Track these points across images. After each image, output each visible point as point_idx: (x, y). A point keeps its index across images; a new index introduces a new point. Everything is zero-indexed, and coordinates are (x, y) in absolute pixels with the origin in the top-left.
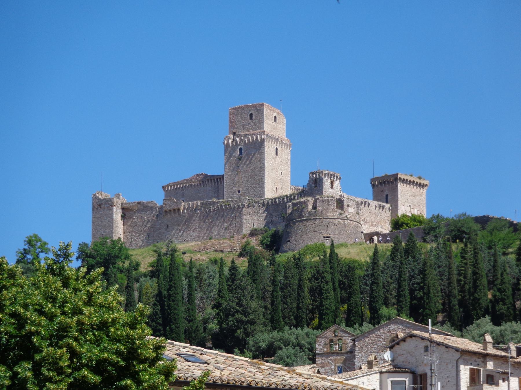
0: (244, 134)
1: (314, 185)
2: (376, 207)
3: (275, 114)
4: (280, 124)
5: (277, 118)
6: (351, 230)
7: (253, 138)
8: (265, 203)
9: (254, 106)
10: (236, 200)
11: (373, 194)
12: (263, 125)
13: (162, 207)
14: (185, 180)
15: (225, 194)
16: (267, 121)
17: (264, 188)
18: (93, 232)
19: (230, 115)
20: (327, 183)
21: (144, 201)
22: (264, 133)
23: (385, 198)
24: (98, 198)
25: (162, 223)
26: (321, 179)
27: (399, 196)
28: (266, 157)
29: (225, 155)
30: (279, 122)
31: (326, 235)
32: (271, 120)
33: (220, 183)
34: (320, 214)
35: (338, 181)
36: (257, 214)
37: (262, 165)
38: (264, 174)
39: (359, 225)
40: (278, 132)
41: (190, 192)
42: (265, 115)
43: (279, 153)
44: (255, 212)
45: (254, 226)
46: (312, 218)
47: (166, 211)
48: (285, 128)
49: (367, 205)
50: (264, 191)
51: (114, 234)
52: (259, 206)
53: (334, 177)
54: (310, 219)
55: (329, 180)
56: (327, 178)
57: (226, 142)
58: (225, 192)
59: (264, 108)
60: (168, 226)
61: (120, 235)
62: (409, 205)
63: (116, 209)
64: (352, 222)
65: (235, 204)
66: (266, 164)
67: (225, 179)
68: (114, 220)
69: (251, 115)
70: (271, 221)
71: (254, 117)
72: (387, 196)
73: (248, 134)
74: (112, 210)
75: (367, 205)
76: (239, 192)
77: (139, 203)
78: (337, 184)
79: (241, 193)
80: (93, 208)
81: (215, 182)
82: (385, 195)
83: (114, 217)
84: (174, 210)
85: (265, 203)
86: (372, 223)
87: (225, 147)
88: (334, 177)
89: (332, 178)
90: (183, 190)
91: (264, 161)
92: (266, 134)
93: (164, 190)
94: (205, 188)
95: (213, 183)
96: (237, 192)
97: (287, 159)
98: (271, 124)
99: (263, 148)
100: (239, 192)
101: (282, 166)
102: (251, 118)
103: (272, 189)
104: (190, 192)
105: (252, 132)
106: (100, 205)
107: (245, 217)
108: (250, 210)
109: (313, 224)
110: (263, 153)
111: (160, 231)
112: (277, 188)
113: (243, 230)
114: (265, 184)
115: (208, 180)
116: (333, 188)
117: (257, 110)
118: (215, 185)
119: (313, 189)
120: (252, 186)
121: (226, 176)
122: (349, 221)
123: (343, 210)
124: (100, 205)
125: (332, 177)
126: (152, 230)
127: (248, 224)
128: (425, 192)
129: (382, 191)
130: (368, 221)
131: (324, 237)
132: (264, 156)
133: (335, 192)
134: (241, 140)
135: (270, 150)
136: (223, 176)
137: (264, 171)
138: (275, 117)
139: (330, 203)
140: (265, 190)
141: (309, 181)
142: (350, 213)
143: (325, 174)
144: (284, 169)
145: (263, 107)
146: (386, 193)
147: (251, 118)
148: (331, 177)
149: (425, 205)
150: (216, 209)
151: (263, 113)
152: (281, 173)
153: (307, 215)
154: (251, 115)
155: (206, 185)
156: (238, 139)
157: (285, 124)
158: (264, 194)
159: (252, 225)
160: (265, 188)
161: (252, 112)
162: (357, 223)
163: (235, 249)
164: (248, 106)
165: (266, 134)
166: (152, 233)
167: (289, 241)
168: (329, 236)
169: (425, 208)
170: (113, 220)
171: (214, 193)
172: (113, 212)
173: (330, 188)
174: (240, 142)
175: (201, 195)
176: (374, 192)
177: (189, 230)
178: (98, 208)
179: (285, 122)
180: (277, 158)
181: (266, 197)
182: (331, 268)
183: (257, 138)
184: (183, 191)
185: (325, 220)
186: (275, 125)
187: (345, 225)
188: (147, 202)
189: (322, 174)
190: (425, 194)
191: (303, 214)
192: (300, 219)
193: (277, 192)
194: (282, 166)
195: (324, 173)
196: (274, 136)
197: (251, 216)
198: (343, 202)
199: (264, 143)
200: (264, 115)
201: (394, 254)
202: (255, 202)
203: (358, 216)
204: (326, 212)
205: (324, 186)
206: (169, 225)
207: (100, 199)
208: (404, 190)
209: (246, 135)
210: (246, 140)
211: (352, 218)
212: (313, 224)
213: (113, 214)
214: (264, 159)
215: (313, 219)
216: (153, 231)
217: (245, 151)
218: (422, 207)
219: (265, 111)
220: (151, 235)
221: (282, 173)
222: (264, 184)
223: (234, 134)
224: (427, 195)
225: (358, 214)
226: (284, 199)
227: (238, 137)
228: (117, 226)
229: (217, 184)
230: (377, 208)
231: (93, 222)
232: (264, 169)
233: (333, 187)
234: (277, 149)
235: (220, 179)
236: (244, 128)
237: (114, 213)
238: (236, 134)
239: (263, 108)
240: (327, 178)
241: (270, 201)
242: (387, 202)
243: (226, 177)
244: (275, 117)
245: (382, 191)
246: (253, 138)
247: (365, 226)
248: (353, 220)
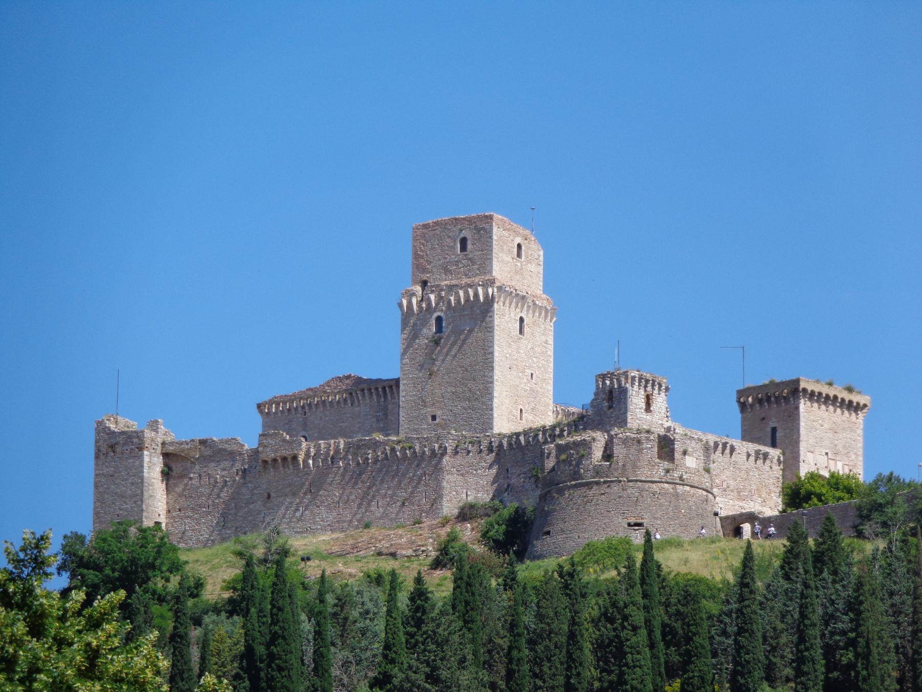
0: (446, 285)
1: (607, 404)
2: (748, 455)
3: (518, 240)
4: (529, 262)
5: (523, 248)
6: (690, 509)
7: (466, 293)
8: (495, 445)
9: (470, 220)
10: (428, 437)
11: (743, 425)
12: (491, 263)
13: (256, 452)
14: (311, 389)
15: (401, 422)
16: (501, 255)
17: (492, 410)
18: (95, 508)
19: (415, 239)
20: (636, 398)
21: (215, 439)
22: (492, 282)
23: (770, 435)
24: (109, 430)
25: (256, 488)
26: (623, 391)
27: (803, 431)
28: (496, 337)
29: (402, 333)
30: (527, 257)
31: (633, 521)
32: (510, 252)
33: (389, 398)
34: (620, 471)
35: (663, 394)
36: (475, 470)
37: (489, 356)
38: (492, 377)
39: (710, 496)
40: (525, 281)
41: (321, 419)
42: (496, 240)
43: (526, 329)
45: (469, 498)
46: (602, 480)
47: (265, 462)
48: (542, 272)
49: (728, 451)
50: (491, 418)
51: (145, 514)
52: (481, 451)
53: (653, 385)
54: (597, 483)
55: (642, 391)
56: (636, 387)
57: (405, 302)
58: (401, 419)
59: (494, 224)
60: (269, 496)
61: (159, 515)
62: (824, 451)
63: (151, 456)
64: (693, 490)
65: (425, 447)
66: (496, 354)
67: (402, 387)
68: (145, 481)
69: (464, 242)
70: (509, 486)
71: (469, 246)
72: (774, 430)
73: (457, 285)
74: (141, 458)
75: (728, 451)
76: (434, 418)
77: (203, 442)
78: (660, 401)
79: (438, 421)
80: (96, 453)
81: (378, 395)
82: (769, 429)
83: (146, 475)
84: (284, 459)
85: (495, 445)
86: (739, 492)
87: (403, 314)
88: (653, 385)
89: (649, 388)
90: (305, 412)
91: (492, 347)
92: (498, 284)
93: (261, 412)
94: (356, 409)
95: (375, 397)
96: (430, 418)
97: (546, 342)
98: (509, 262)
99: (491, 317)
100: (434, 418)
101: (535, 359)
102: (464, 247)
103: (511, 412)
104: (321, 419)
105: (465, 280)
106: (112, 447)
108: (459, 460)
109: (604, 494)
110: (490, 329)
111: (251, 506)
112: (521, 410)
113: (444, 507)
114: (495, 400)
115: (363, 390)
116: (650, 411)
117: (478, 230)
118: (378, 401)
119: (605, 414)
120: (466, 404)
121: (405, 382)
122: (688, 488)
123: (674, 463)
124: (112, 447)
125: (649, 385)
126: (233, 505)
128: (861, 421)
129: (764, 419)
130: (731, 488)
131: (629, 525)
132: (493, 337)
133: (654, 420)
134: (440, 298)
135: (507, 322)
136: (397, 381)
137: (493, 370)
138: (519, 246)
139: (644, 446)
140: (495, 415)
141: (596, 394)
142: (689, 468)
143: (633, 378)
144: (539, 367)
145: (492, 223)
146: (774, 425)
147: (464, 247)
148: (646, 387)
149: (861, 452)
150: (380, 459)
151: (491, 237)
152: (532, 374)
153: (589, 474)
154: (464, 242)
155: (359, 401)
156: (432, 297)
157: (542, 263)
158: (492, 424)
159: (464, 496)
160: (495, 409)
161: (465, 233)
162: (705, 493)
163: (423, 551)
164: (456, 219)
165: (498, 284)
166: (232, 512)
167: (548, 533)
168: (640, 521)
169: (861, 458)
170: (142, 483)
171: (378, 420)
172: (142, 461)
173: (643, 411)
174: (437, 304)
175: (346, 424)
176: (744, 420)
177: (318, 507)
178: (107, 453)
179: (542, 258)
180: (524, 341)
181: (496, 430)
182: (645, 596)
183: (476, 295)
184: (305, 415)
185: (631, 484)
186: (519, 264)
187: (676, 495)
188: (221, 441)
189: (627, 378)
190: (862, 426)
191: (582, 471)
192: (573, 483)
193: (521, 418)
194: (535, 359)
195: (630, 377)
196: (516, 290)
197: (462, 475)
198: (673, 444)
199: (492, 306)
200: (494, 242)
201: (789, 563)
202: (470, 442)
203: (707, 475)
204: (635, 467)
205: (631, 407)
206: (272, 494)
207: (114, 432)
208: (812, 418)
209: (451, 288)
210: (452, 298)
211: (695, 480)
212: (604, 494)
213: (142, 466)
214: (492, 342)
215: (605, 482)
216: (236, 506)
217: (449, 324)
218: (853, 457)
219: (496, 232)
220: (230, 517)
221: (534, 376)
222: (491, 399)
223: (424, 284)
224: (866, 429)
225: (708, 471)
226: (537, 435)
227: (432, 292)
228: (151, 496)
229: (383, 399)
230: (752, 459)
231: (96, 486)
232: (492, 367)
233: (652, 409)
234: (522, 320)
235: (391, 387)
236: (447, 271)
237: (145, 465)
238: (429, 284)
239: (491, 226)
240: (636, 387)
241: (506, 439)
242: (774, 445)
243: (404, 385)
244: (519, 246)
245: (764, 419)
246: (466, 293)
247: (722, 499)
248: (696, 485)
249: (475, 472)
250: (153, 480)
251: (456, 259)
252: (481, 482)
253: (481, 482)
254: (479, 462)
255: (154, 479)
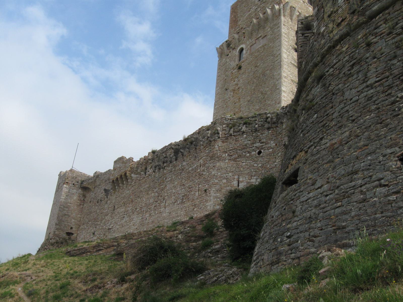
36: (249, 152)
44: (244, 147)
61: (71, 228)
107: (218, 164)
108: (232, 144)
127: (225, 181)
159: (235, 183)
197: (235, 160)
202: (245, 123)
206: (116, 207)
228: (65, 215)
249: (248, 155)
250: (69, 204)
251: (256, 7)
252: (255, 165)
253: (255, 165)
254: (253, 143)
255: (70, 203)
